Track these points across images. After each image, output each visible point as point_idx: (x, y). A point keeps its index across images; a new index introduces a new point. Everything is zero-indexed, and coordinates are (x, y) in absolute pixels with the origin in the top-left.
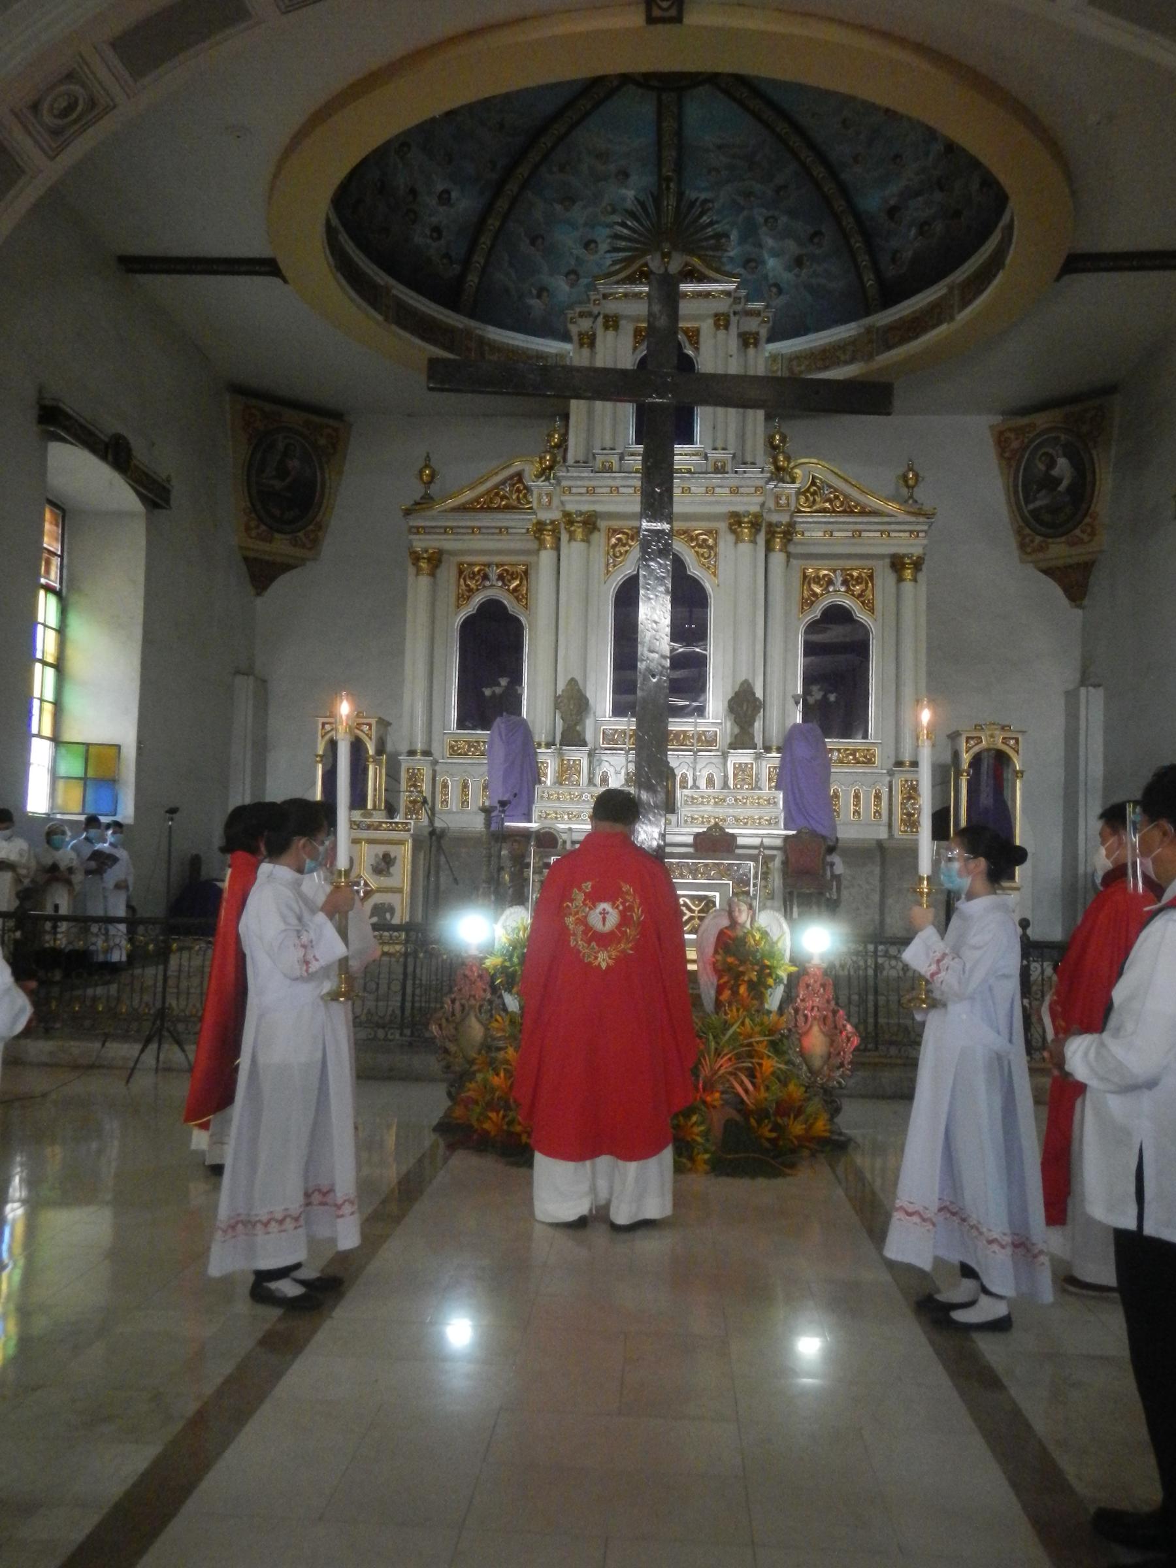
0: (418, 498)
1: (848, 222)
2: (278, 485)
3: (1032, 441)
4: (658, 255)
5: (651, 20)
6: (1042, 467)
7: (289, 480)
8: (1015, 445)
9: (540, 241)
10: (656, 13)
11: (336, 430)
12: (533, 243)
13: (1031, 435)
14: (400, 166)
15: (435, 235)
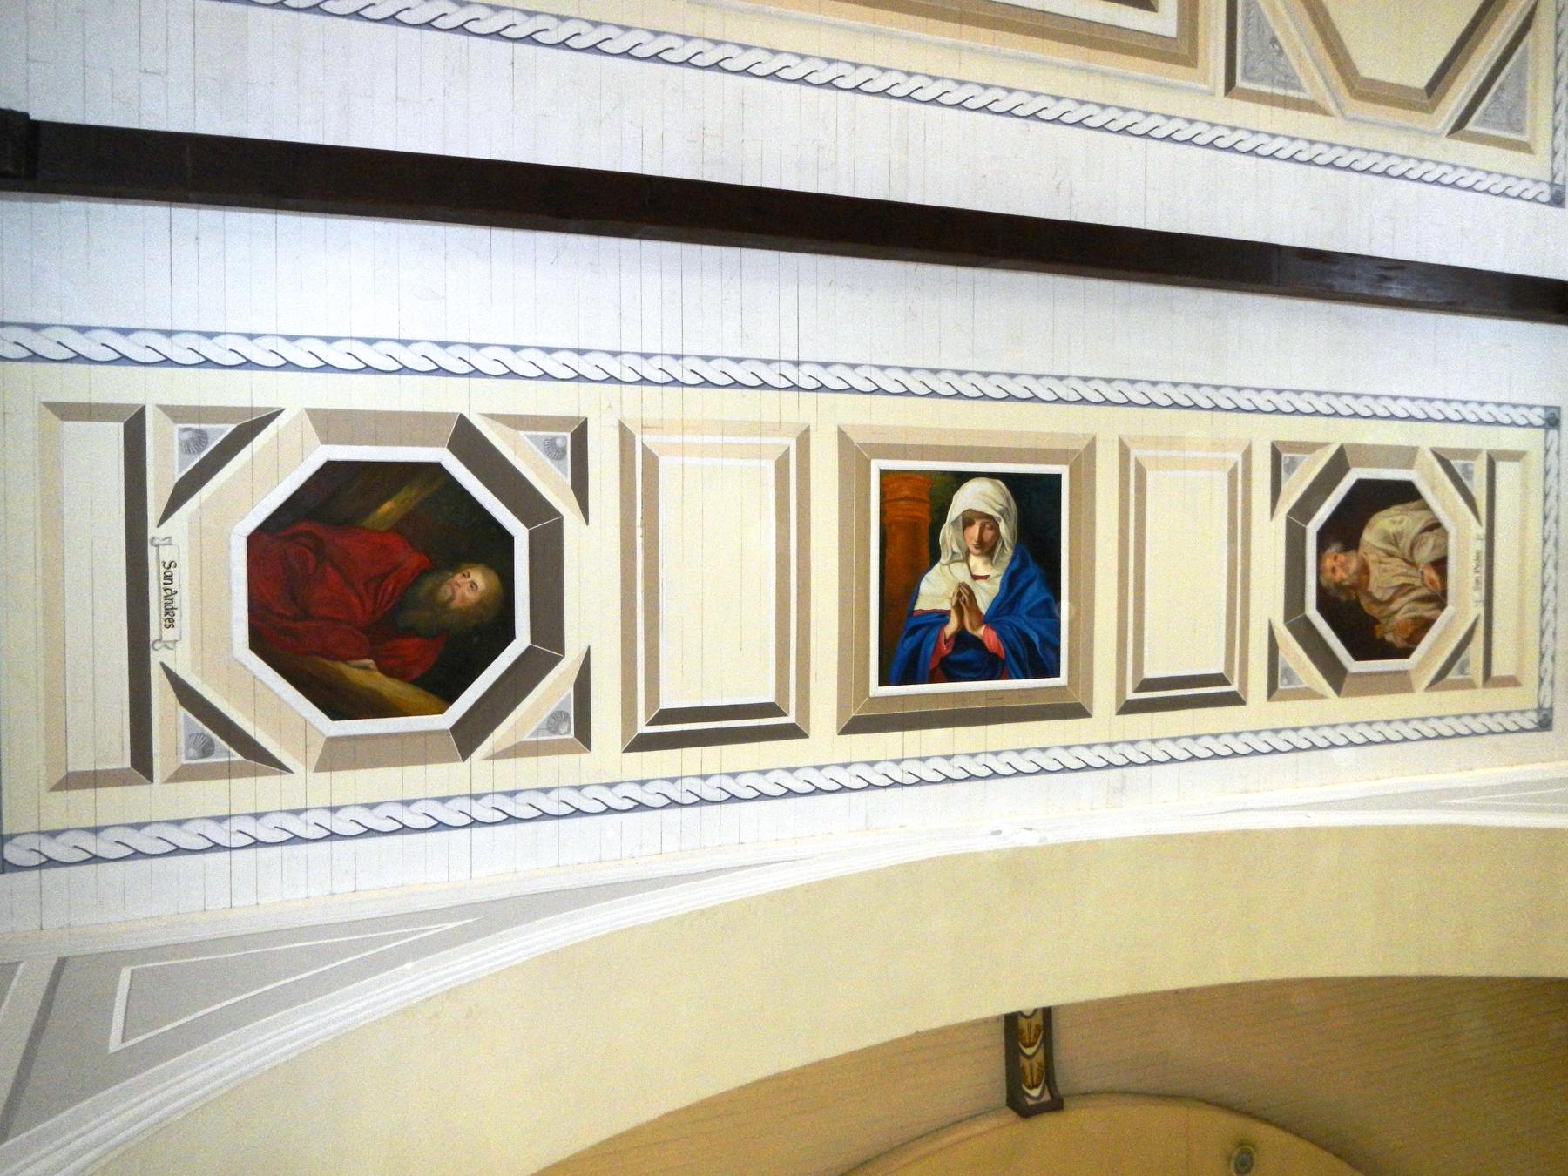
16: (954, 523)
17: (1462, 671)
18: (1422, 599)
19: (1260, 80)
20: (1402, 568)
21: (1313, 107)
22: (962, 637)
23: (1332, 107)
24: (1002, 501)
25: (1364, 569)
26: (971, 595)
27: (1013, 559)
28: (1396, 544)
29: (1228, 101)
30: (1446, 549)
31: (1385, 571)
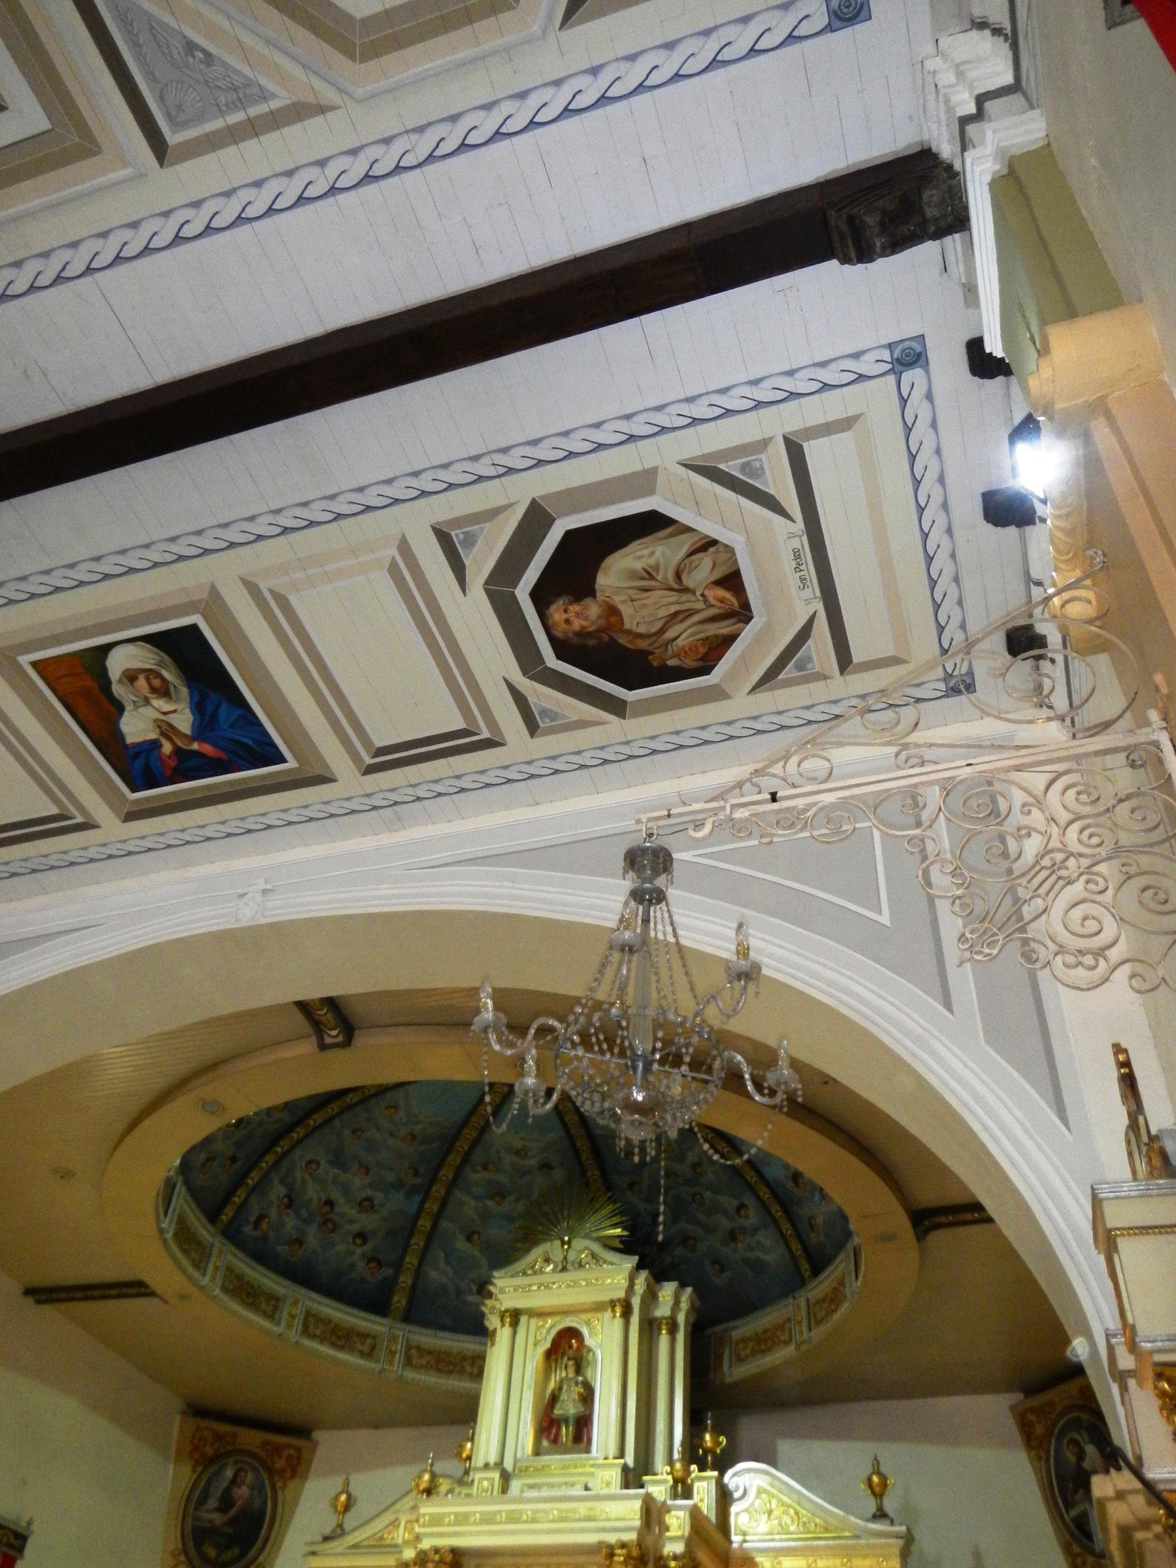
0: (327, 1531)
1: (764, 1192)
2: (217, 1518)
3: (1054, 1425)
4: (558, 1243)
5: (323, 1047)
6: (1073, 1459)
7: (233, 1511)
8: (1039, 1429)
9: (476, 1236)
10: (328, 1040)
11: (298, 1450)
12: (469, 1238)
13: (1053, 1416)
14: (310, 1184)
15: (358, 1241)
16: (120, 681)
17: (800, 667)
18: (713, 619)
19: (200, 118)
20: (673, 597)
21: (299, 112)
22: (178, 752)
23: (330, 95)
24: (152, 656)
25: (612, 611)
26: (170, 725)
27: (191, 694)
28: (651, 577)
29: (169, 172)
30: (736, 562)
31: (645, 606)
